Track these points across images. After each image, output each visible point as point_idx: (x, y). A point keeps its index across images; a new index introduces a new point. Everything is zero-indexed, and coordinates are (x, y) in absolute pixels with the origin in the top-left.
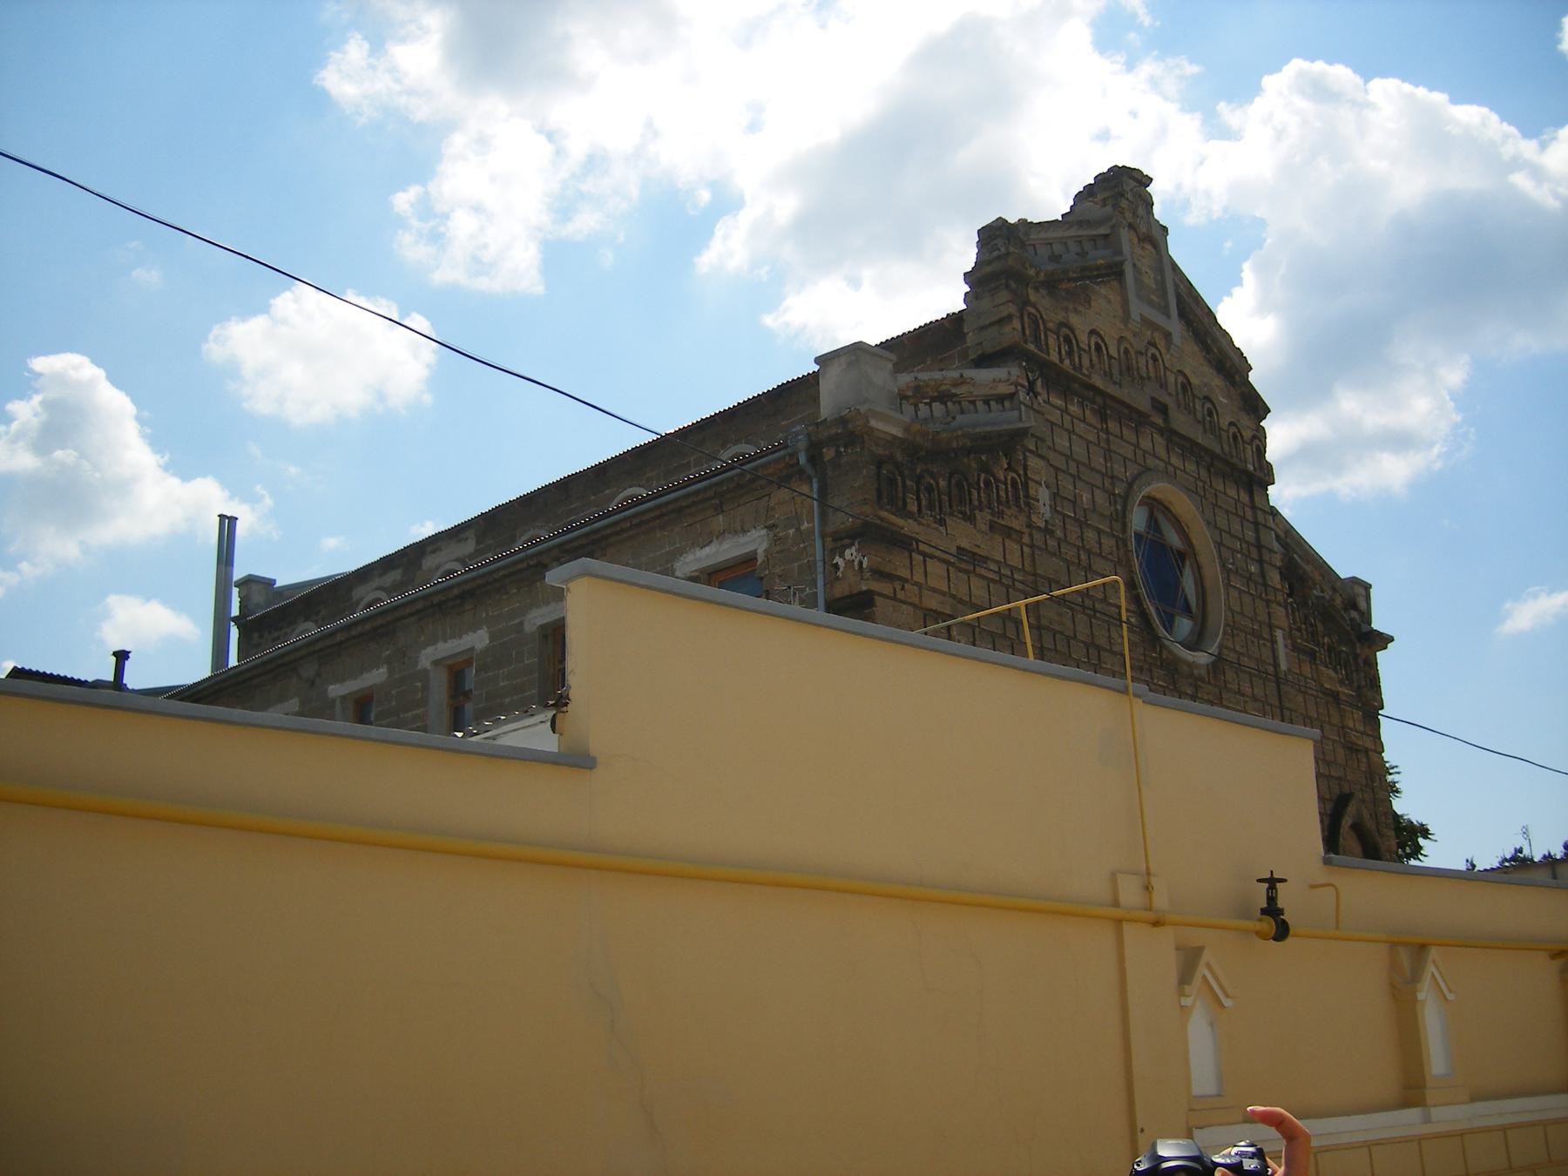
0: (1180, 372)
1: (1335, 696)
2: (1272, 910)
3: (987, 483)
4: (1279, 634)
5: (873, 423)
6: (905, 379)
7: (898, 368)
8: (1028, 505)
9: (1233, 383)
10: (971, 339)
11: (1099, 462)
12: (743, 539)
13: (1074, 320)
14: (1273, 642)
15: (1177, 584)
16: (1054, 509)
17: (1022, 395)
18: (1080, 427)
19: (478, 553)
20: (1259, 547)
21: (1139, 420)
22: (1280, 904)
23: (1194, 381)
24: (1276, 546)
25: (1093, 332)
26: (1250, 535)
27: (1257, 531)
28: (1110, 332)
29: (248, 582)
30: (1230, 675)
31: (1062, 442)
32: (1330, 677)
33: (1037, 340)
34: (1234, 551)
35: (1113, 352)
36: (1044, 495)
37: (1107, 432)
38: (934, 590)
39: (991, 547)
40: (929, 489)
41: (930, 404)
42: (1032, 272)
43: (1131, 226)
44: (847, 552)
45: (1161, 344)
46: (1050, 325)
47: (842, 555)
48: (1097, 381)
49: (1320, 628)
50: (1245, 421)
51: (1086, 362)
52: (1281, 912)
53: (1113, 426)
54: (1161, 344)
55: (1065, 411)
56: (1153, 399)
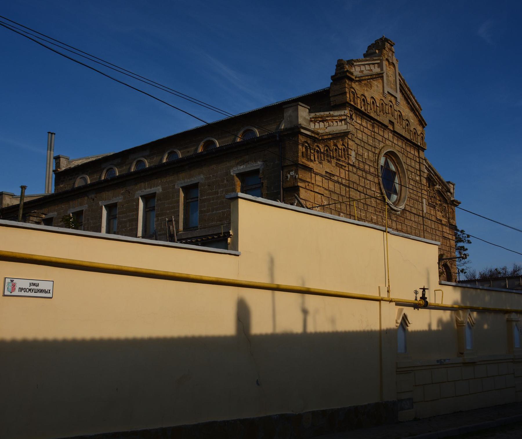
0: (399, 111)
1: (441, 221)
2: (423, 298)
3: (336, 149)
4: (424, 200)
5: (302, 131)
7: (310, 112)
8: (348, 157)
9: (416, 115)
10: (332, 99)
13: (366, 94)
14: (422, 203)
16: (356, 158)
17: (348, 120)
18: (366, 130)
20: (420, 170)
21: (385, 127)
23: (403, 114)
24: (426, 171)
25: (372, 98)
26: (417, 167)
27: (420, 166)
28: (378, 97)
31: (360, 136)
32: (439, 215)
33: (354, 101)
34: (412, 172)
35: (378, 105)
36: (353, 154)
37: (374, 132)
38: (318, 186)
39: (336, 171)
40: (318, 152)
41: (319, 123)
42: (354, 78)
43: (387, 60)
44: (292, 173)
45: (394, 101)
46: (359, 96)
47: (289, 173)
48: (372, 115)
49: (438, 198)
51: (369, 108)
52: (426, 298)
53: (376, 130)
54: (394, 101)
55: (361, 125)
56: (390, 121)
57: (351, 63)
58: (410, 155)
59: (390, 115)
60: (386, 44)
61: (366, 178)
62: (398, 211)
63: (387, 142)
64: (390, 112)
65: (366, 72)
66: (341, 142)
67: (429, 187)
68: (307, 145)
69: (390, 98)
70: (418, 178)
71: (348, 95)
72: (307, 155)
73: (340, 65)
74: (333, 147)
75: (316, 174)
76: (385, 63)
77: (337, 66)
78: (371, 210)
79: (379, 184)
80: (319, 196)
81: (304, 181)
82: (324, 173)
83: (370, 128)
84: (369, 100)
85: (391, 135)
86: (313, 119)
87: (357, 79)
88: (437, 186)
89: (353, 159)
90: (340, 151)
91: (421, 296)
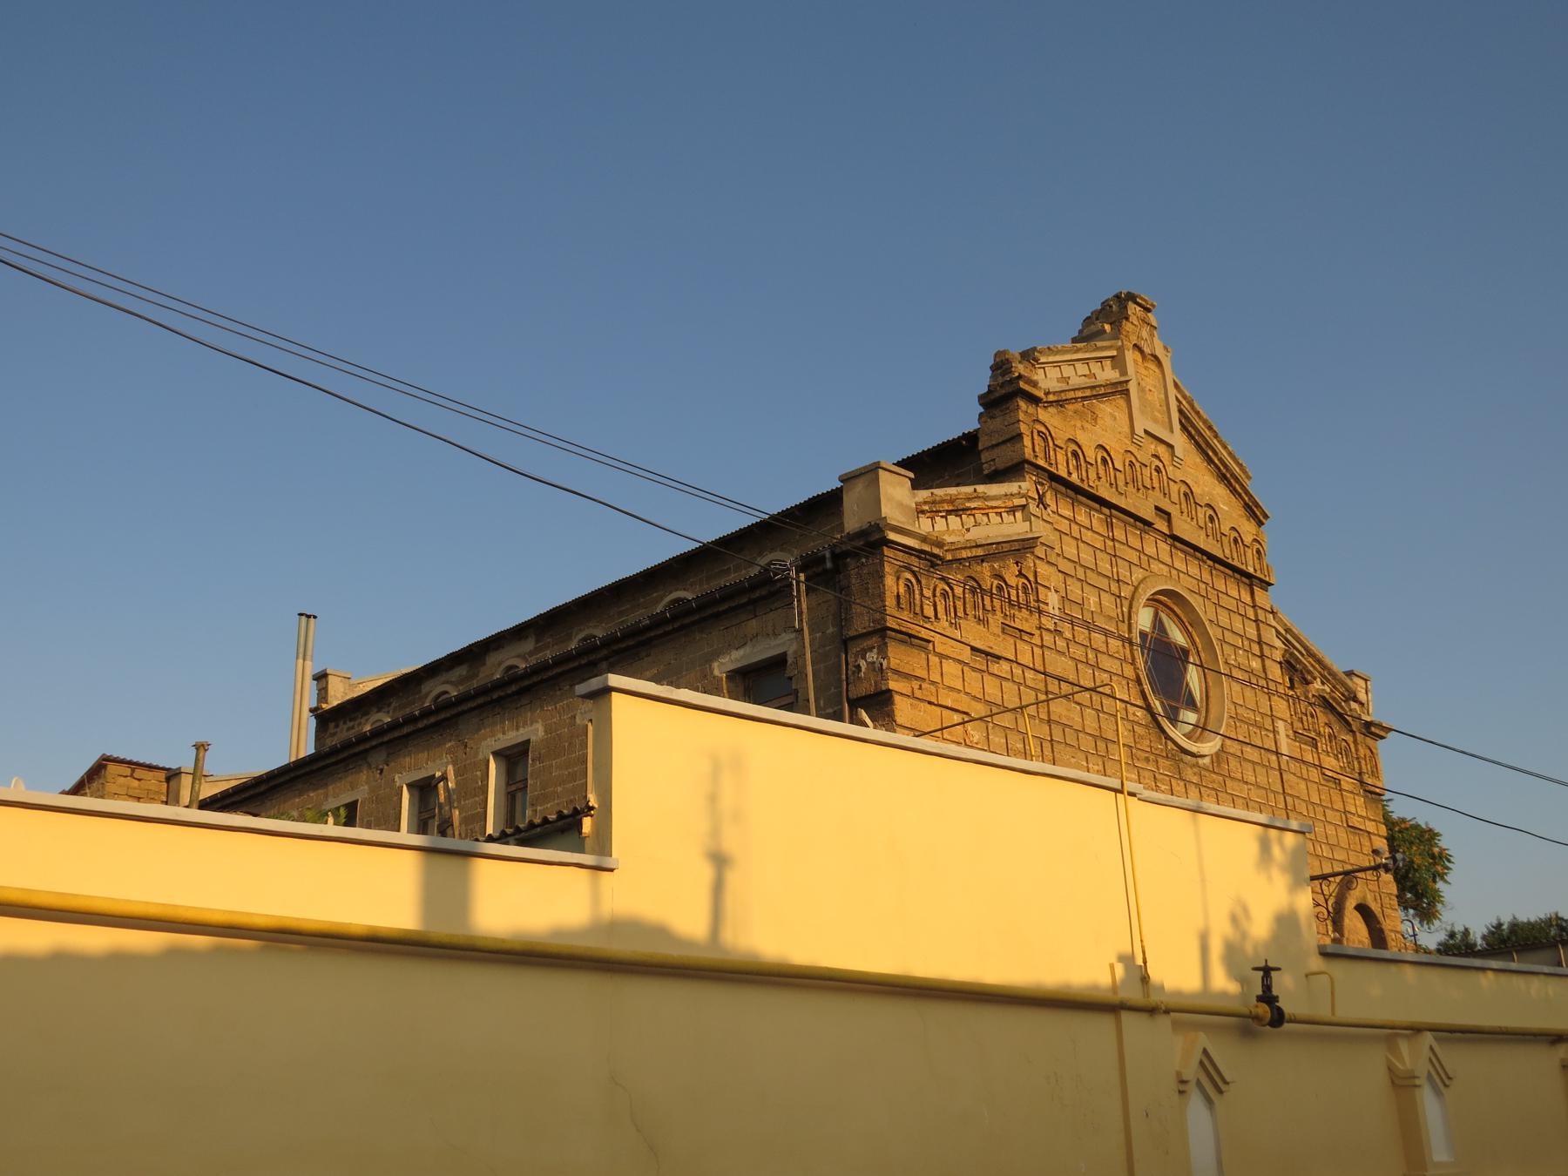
2: (1268, 997)
3: (1000, 588)
4: (1280, 725)
5: (892, 536)
7: (916, 485)
9: (1234, 491)
10: (985, 457)
11: (1105, 566)
12: (773, 643)
13: (1081, 438)
14: (1275, 732)
17: (1033, 507)
18: (1087, 536)
19: (536, 650)
22: (1275, 992)
24: (1278, 643)
25: (1101, 447)
26: (1252, 632)
27: (1258, 629)
28: (1116, 447)
30: (1233, 763)
31: (1070, 550)
33: (1047, 458)
35: (1118, 465)
38: (951, 689)
39: (1004, 647)
40: (945, 595)
42: (1040, 394)
44: (872, 656)
47: (864, 658)
48: (1105, 492)
49: (1322, 718)
51: (1092, 476)
52: (1276, 999)
53: (1119, 534)
55: (1073, 521)
56: (1157, 508)
58: (1224, 601)
59: (1157, 493)
60: (1131, 305)
62: (1203, 756)
63: (1155, 566)
64: (1156, 485)
65: (1076, 381)
66: (1015, 570)
67: (1292, 687)
68: (908, 575)
69: (1153, 447)
70: (1255, 664)
71: (1027, 441)
72: (911, 604)
73: (1001, 366)
75: (942, 656)
76: (1131, 356)
77: (994, 368)
79: (1138, 681)
81: (908, 676)
83: (1102, 530)
84: (1091, 454)
85: (1162, 545)
86: (926, 508)
87: (1051, 398)
88: (1317, 685)
90: (1013, 592)
91: (1260, 992)
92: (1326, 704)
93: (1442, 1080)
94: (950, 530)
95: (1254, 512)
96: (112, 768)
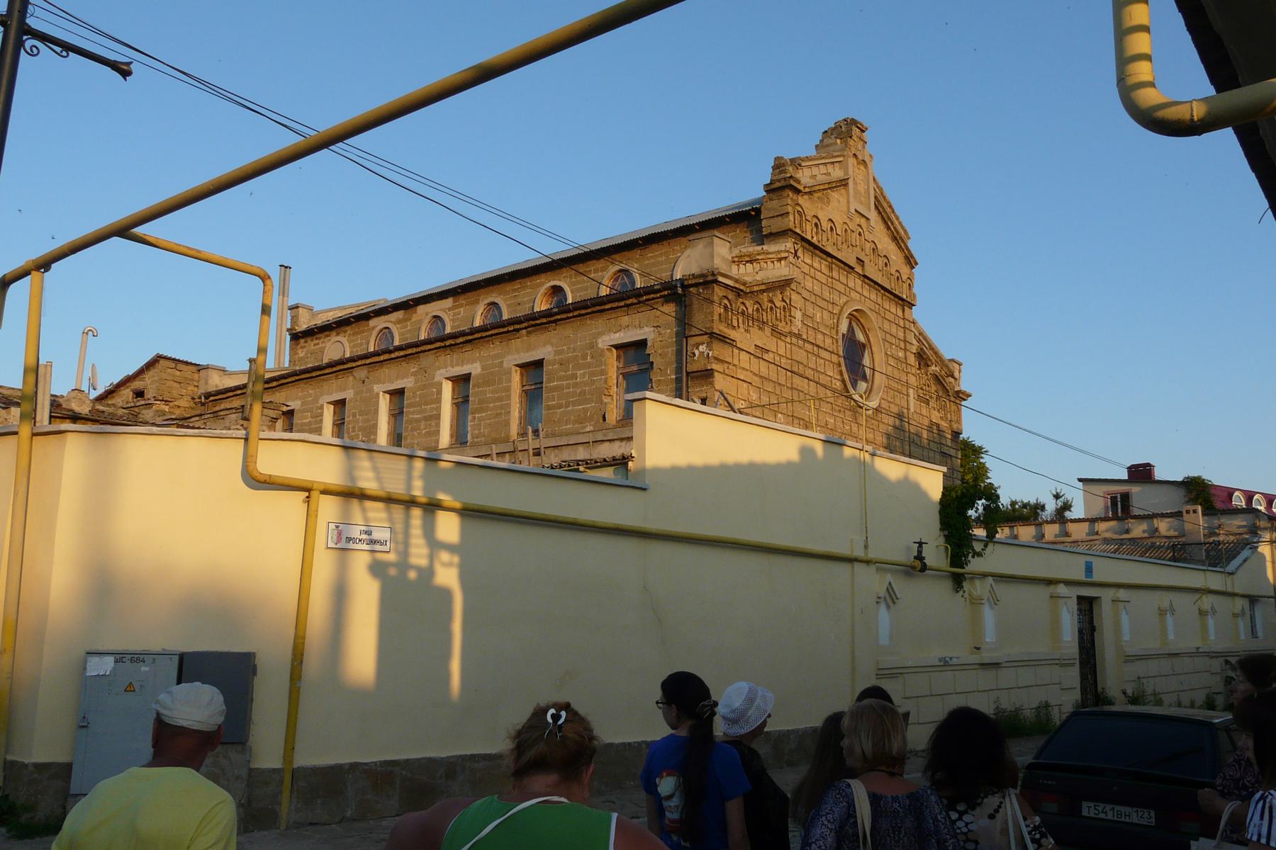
2: (920, 557)
4: (911, 391)
5: (721, 279)
6: (736, 252)
9: (900, 247)
10: (764, 223)
12: (639, 331)
15: (860, 364)
18: (819, 275)
20: (905, 341)
24: (914, 342)
26: (901, 335)
28: (838, 220)
29: (294, 308)
31: (809, 285)
36: (798, 315)
42: (801, 188)
44: (702, 348)
45: (864, 225)
48: (829, 250)
49: (934, 388)
50: (905, 270)
53: (835, 274)
55: (812, 266)
57: (797, 163)
58: (888, 316)
60: (854, 128)
61: (818, 356)
63: (853, 294)
65: (821, 179)
69: (858, 220)
70: (901, 354)
71: (791, 217)
72: (726, 319)
73: (779, 165)
74: (767, 305)
76: (852, 161)
77: (774, 168)
78: (826, 408)
79: (839, 365)
80: (745, 385)
81: (722, 361)
82: (752, 350)
84: (826, 225)
85: (859, 282)
88: (933, 368)
89: (798, 324)
92: (937, 379)
93: (995, 601)
94: (747, 273)
95: (910, 261)
96: (162, 362)
